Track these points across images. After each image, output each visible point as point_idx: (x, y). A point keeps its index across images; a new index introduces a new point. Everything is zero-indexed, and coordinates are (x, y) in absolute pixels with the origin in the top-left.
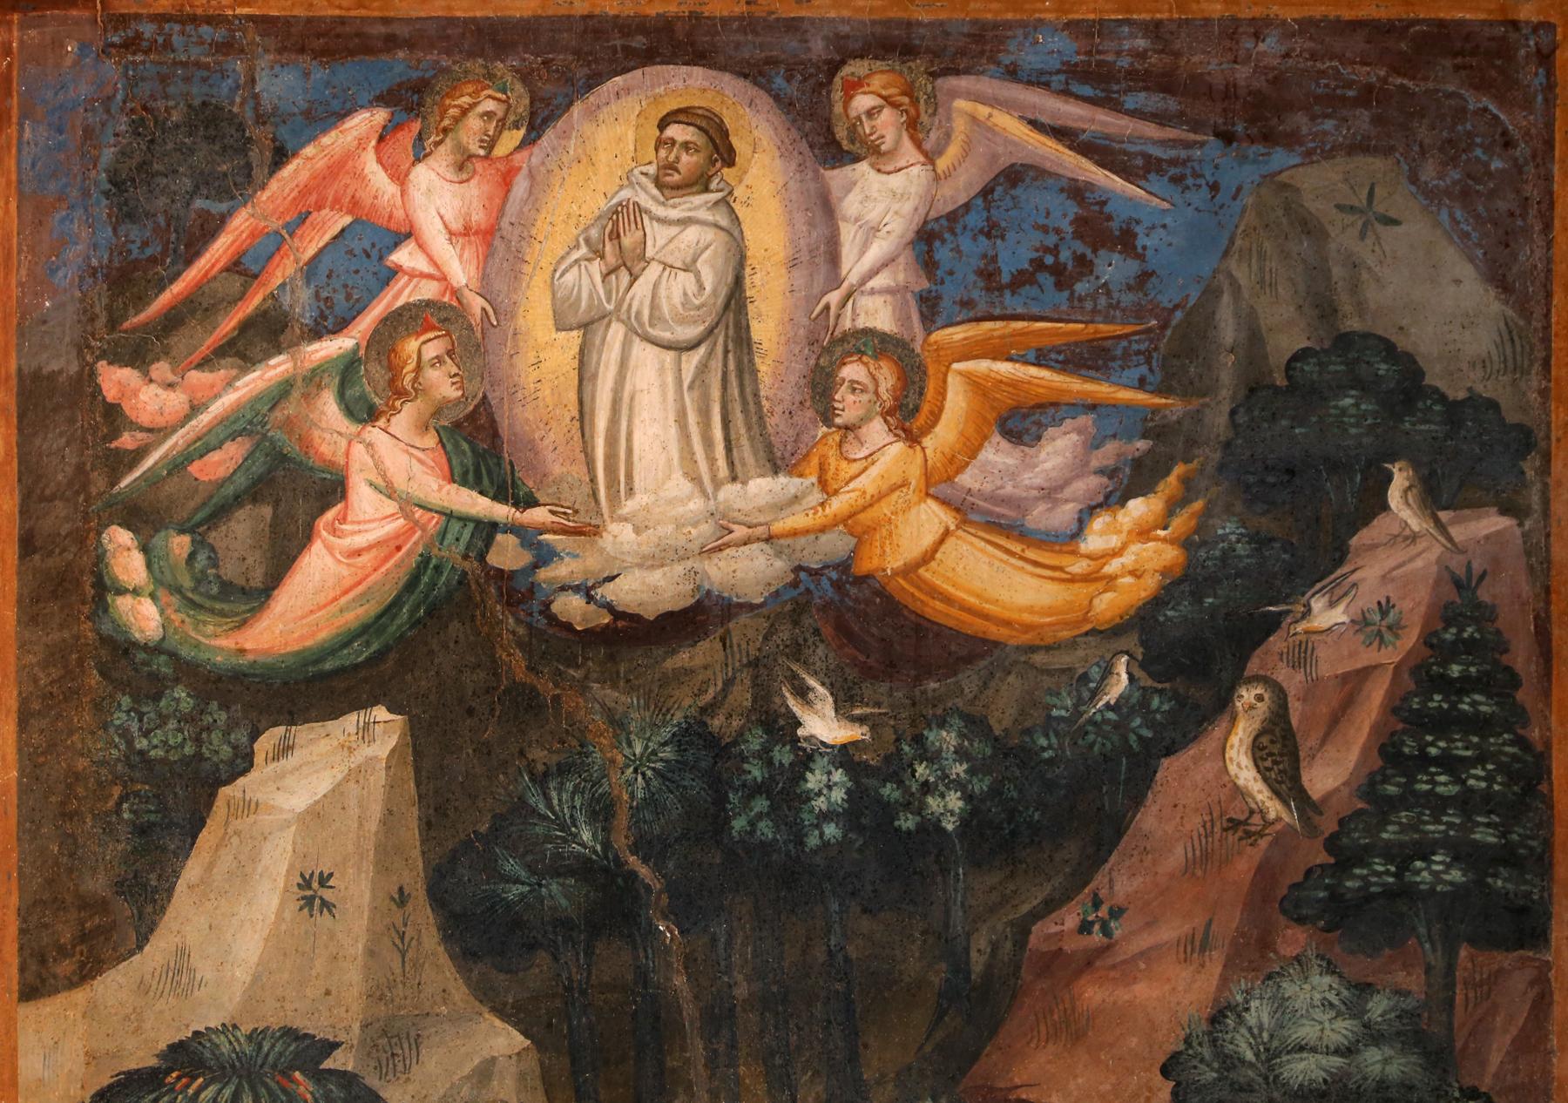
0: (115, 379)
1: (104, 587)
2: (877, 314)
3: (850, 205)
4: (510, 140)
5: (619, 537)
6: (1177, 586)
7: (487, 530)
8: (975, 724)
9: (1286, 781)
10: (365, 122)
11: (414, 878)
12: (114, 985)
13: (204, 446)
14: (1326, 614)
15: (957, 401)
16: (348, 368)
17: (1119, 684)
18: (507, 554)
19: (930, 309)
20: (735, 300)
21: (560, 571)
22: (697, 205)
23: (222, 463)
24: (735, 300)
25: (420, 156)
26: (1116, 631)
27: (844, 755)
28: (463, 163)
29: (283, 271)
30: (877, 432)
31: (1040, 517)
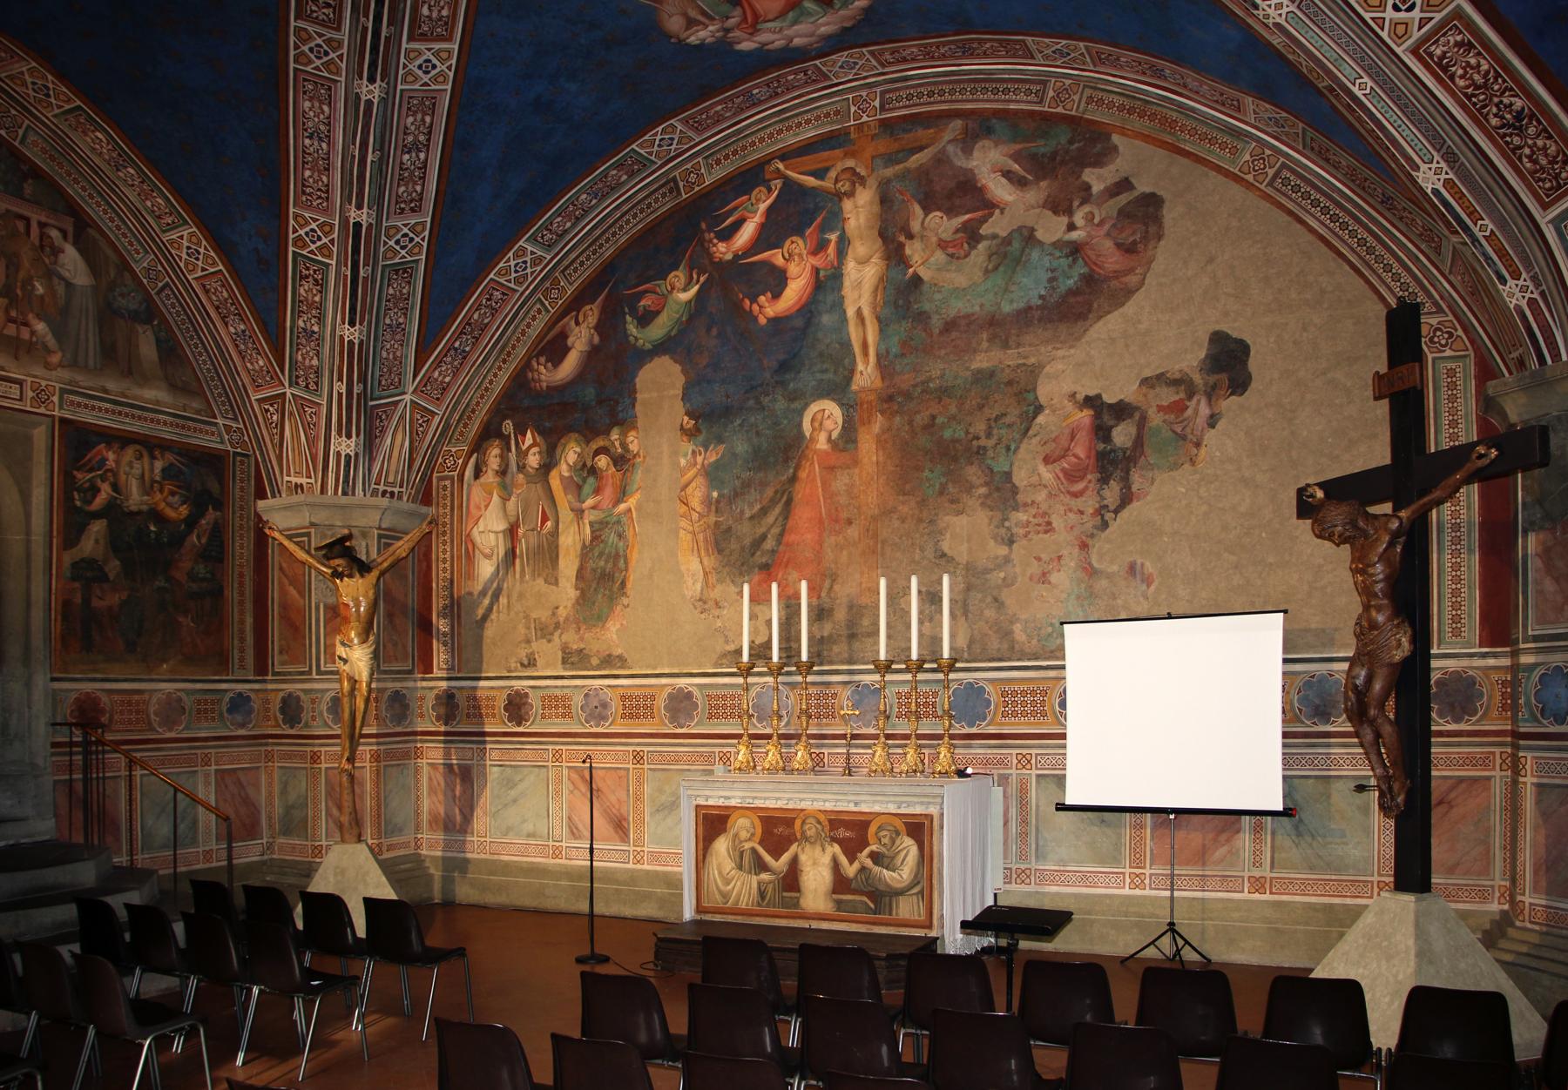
0: (75, 473)
1: (74, 499)
2: (158, 478)
5: (131, 501)
6: (189, 516)
7: (116, 498)
9: (200, 542)
10: (103, 445)
12: (74, 550)
13: (85, 483)
15: (166, 491)
16: (101, 476)
17: (183, 526)
18: (118, 502)
19: (164, 479)
20: (143, 475)
21: (125, 504)
23: (87, 485)
24: (143, 475)
26: (181, 521)
28: (114, 452)
29: (94, 462)
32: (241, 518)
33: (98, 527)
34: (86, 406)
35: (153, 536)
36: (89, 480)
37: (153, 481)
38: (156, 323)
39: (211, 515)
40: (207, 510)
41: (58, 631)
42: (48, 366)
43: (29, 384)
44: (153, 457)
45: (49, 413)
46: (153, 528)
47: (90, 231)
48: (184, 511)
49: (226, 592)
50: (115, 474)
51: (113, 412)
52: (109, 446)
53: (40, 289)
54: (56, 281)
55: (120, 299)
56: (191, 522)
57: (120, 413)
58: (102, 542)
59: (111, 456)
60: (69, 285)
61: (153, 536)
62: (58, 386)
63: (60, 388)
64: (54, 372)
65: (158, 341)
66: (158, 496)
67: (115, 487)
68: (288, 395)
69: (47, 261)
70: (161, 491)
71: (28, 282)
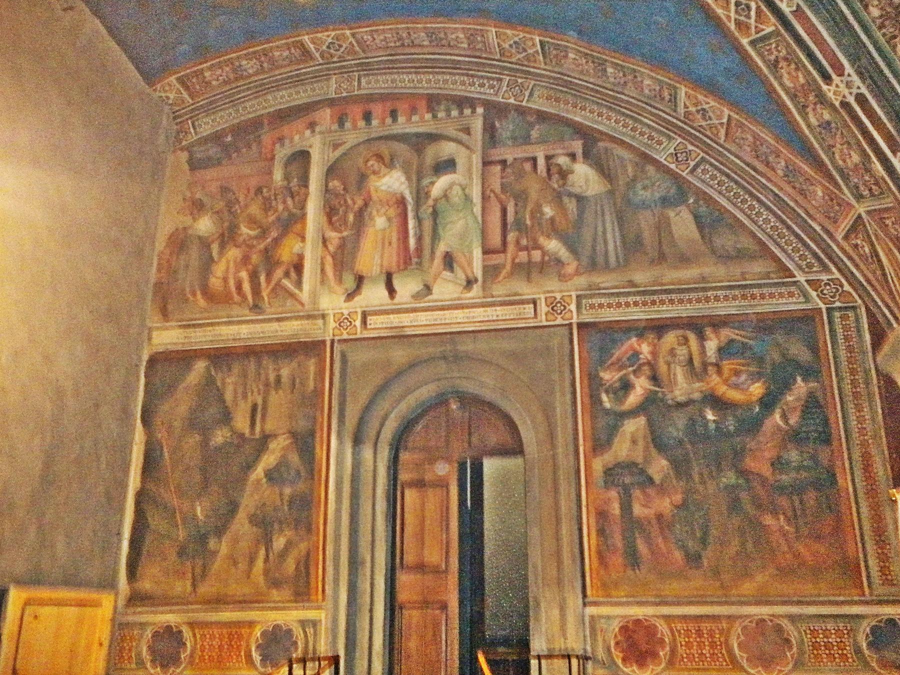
3: (707, 346)
4: (656, 341)
5: (677, 393)
7: (658, 392)
8: (735, 416)
9: (787, 423)
11: (650, 440)
14: (790, 398)
18: (660, 395)
22: (684, 347)
23: (617, 385)
25: (643, 343)
27: (714, 421)
28: (649, 344)
30: (714, 376)
31: (741, 386)
32: (854, 383)
33: (634, 426)
34: (610, 306)
35: (712, 426)
36: (621, 379)
37: (705, 365)
38: (691, 201)
39: (801, 388)
40: (795, 380)
41: (593, 549)
42: (562, 278)
43: (543, 300)
44: (702, 337)
45: (567, 322)
46: (710, 416)
47: (601, 144)
48: (757, 389)
49: (840, 481)
50: (652, 365)
51: (645, 304)
52: (641, 336)
53: (548, 211)
54: (566, 200)
55: (641, 192)
56: (768, 403)
57: (654, 303)
58: (641, 443)
59: (645, 349)
60: (580, 199)
61: (712, 426)
62: (574, 294)
63: (578, 296)
64: (569, 283)
65: (697, 217)
66: (715, 379)
67: (654, 379)
68: (864, 215)
69: (556, 186)
70: (719, 372)
71: (538, 209)
